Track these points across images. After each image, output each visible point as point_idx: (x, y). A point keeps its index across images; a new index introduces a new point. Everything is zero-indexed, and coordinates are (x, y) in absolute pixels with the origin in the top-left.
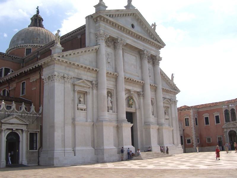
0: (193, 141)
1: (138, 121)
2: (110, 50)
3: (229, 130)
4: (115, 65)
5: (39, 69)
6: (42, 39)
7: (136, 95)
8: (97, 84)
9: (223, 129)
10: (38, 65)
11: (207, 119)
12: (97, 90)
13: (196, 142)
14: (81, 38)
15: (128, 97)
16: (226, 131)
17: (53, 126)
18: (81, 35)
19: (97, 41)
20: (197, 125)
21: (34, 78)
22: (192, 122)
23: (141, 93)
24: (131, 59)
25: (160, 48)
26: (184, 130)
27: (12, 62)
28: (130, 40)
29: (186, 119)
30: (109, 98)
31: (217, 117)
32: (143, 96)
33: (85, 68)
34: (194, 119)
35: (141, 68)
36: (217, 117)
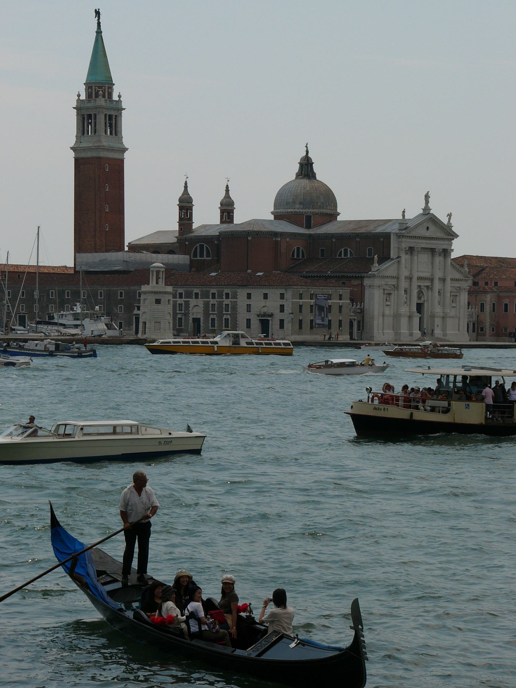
2: (408, 256)
4: (411, 268)
5: (362, 278)
6: (323, 203)
7: (425, 289)
8: (398, 286)
12: (398, 291)
14: (383, 241)
15: (419, 291)
18: (384, 239)
19: (399, 253)
20: (494, 311)
21: (356, 282)
22: (488, 308)
23: (430, 287)
24: (425, 258)
25: (453, 239)
26: (478, 316)
28: (424, 244)
29: (481, 303)
30: (405, 295)
32: (432, 289)
34: (490, 305)
35: (432, 263)
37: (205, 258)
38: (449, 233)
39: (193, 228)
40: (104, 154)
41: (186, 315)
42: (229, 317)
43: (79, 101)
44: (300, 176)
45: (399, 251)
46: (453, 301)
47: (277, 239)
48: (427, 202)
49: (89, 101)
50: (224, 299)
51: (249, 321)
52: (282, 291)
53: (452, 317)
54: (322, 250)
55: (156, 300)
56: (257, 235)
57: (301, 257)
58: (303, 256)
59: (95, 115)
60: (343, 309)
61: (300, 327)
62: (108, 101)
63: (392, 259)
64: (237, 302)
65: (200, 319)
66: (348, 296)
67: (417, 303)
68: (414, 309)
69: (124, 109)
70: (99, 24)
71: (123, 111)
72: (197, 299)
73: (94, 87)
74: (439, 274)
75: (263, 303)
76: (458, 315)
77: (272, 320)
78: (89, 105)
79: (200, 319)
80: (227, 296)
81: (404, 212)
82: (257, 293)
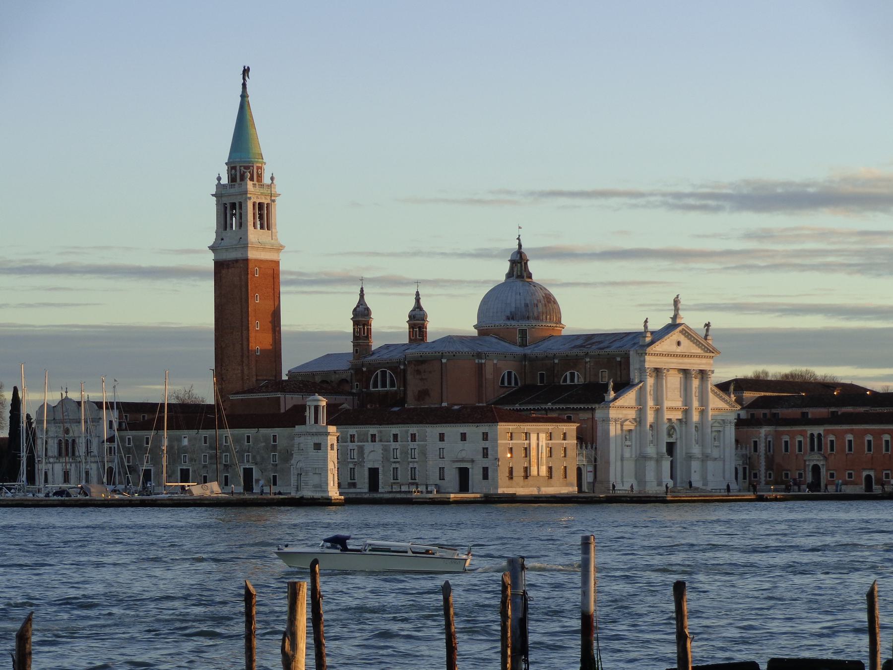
0: (760, 475)
1: (678, 452)
3: (812, 464)
5: (593, 410)
7: (678, 423)
9: (805, 461)
10: (592, 407)
11: (786, 442)
12: (640, 426)
13: (766, 477)
16: (809, 465)
17: (608, 463)
19: (641, 376)
22: (762, 447)
26: (749, 458)
27: (514, 361)
30: (651, 432)
31: (800, 442)
33: (632, 408)
34: (766, 442)
36: (800, 442)
37: (388, 388)
38: (708, 349)
39: (372, 350)
40: (252, 254)
41: (360, 463)
42: (416, 465)
43: (219, 186)
44: (511, 277)
45: (641, 373)
46: (715, 439)
47: (480, 361)
48: (677, 309)
49: (232, 186)
50: (410, 443)
51: (442, 470)
52: (484, 428)
53: (715, 459)
54: (542, 375)
55: (315, 444)
56: (453, 356)
57: (513, 384)
58: (516, 383)
59: (240, 204)
60: (568, 452)
61: (511, 477)
62: (257, 186)
63: (634, 385)
64: (426, 445)
65: (378, 469)
66: (574, 434)
67: (668, 443)
68: (664, 450)
69: (280, 195)
70: (244, 85)
71: (277, 198)
72: (374, 443)
73: (238, 168)
74: (695, 404)
75: (461, 444)
76: (722, 457)
77: (472, 468)
78: (232, 191)
79: (378, 469)
80: (413, 437)
81: (646, 322)
82: (452, 431)
